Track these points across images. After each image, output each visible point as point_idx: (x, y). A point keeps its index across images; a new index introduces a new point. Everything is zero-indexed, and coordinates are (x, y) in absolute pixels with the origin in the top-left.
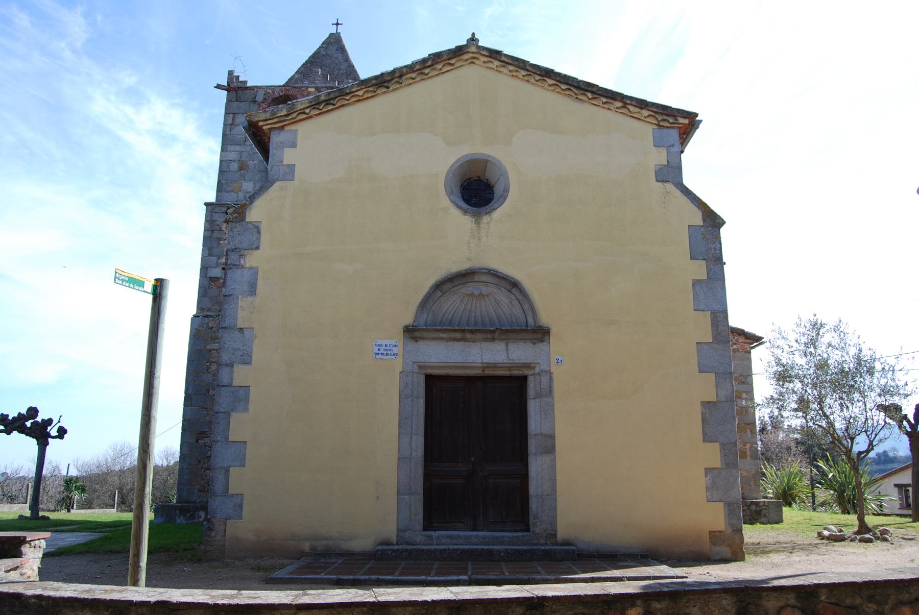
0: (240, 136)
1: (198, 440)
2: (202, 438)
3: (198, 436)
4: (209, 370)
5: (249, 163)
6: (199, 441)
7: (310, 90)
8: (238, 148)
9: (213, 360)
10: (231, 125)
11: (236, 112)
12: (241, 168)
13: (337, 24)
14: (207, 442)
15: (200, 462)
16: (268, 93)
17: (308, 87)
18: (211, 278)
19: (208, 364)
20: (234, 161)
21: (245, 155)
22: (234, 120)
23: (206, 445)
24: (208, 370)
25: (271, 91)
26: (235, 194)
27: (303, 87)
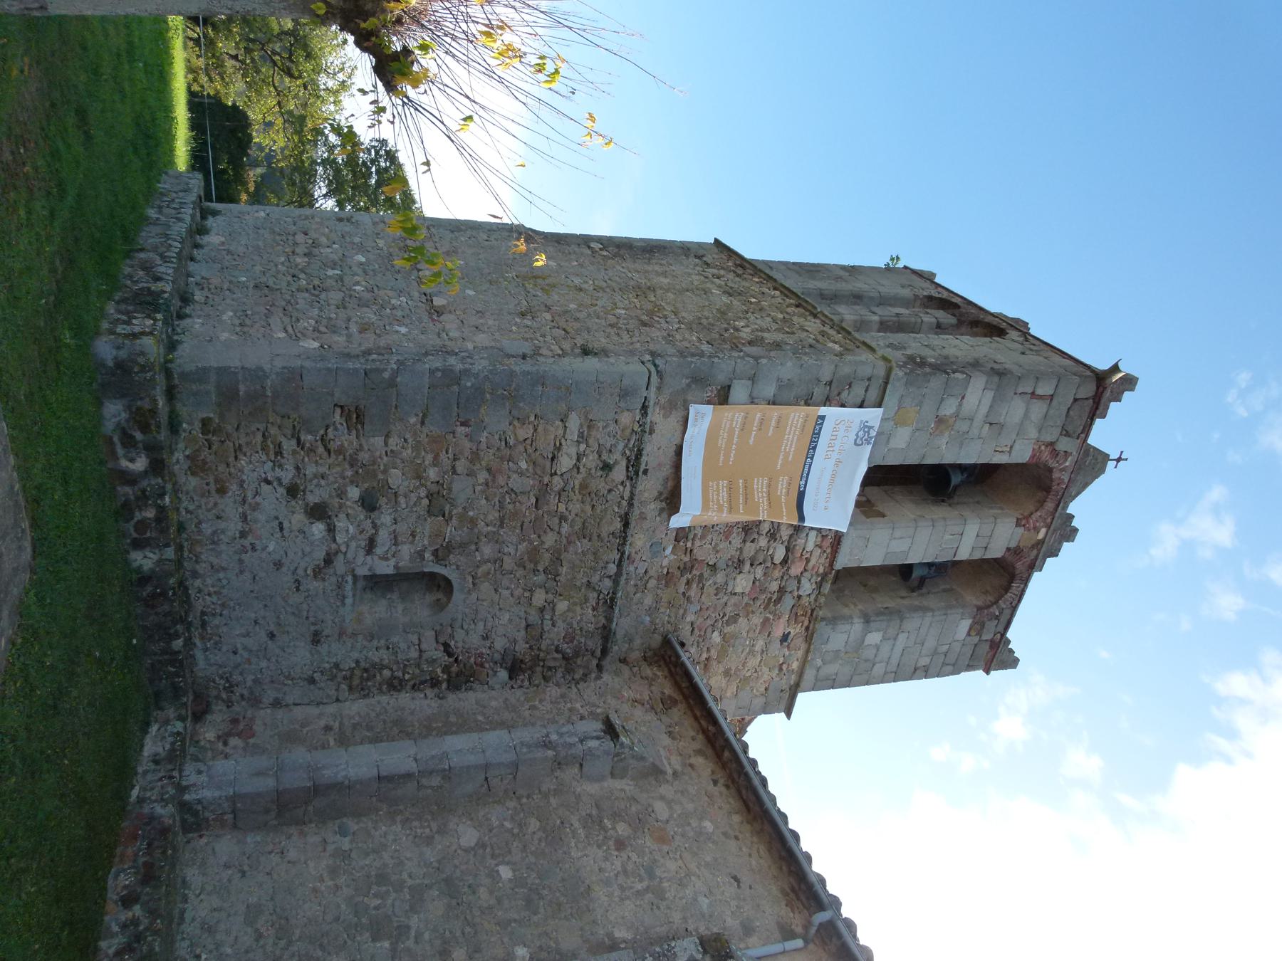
0: (1004, 413)
1: (342, 407)
2: (348, 419)
3: (353, 409)
4: (516, 423)
5: (947, 434)
6: (338, 411)
7: (1043, 531)
8: (984, 410)
9: (540, 429)
10: (1033, 393)
11: (1055, 402)
12: (940, 421)
13: (1119, 460)
14: (336, 429)
15: (283, 417)
16: (1066, 460)
17: (1049, 527)
18: (729, 387)
19: (532, 418)
20: (960, 405)
21: (963, 426)
22: (1041, 397)
23: (327, 427)
24: (518, 419)
25: (1067, 464)
26: (893, 414)
27: (1053, 519)
